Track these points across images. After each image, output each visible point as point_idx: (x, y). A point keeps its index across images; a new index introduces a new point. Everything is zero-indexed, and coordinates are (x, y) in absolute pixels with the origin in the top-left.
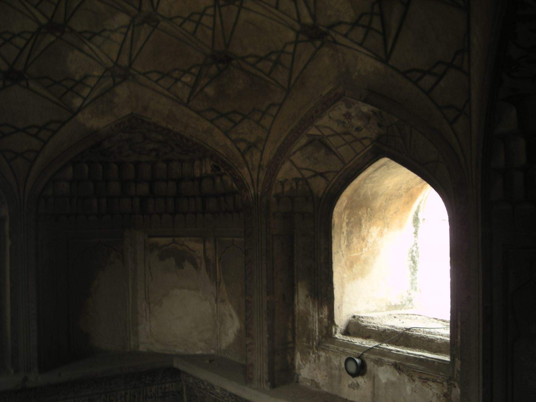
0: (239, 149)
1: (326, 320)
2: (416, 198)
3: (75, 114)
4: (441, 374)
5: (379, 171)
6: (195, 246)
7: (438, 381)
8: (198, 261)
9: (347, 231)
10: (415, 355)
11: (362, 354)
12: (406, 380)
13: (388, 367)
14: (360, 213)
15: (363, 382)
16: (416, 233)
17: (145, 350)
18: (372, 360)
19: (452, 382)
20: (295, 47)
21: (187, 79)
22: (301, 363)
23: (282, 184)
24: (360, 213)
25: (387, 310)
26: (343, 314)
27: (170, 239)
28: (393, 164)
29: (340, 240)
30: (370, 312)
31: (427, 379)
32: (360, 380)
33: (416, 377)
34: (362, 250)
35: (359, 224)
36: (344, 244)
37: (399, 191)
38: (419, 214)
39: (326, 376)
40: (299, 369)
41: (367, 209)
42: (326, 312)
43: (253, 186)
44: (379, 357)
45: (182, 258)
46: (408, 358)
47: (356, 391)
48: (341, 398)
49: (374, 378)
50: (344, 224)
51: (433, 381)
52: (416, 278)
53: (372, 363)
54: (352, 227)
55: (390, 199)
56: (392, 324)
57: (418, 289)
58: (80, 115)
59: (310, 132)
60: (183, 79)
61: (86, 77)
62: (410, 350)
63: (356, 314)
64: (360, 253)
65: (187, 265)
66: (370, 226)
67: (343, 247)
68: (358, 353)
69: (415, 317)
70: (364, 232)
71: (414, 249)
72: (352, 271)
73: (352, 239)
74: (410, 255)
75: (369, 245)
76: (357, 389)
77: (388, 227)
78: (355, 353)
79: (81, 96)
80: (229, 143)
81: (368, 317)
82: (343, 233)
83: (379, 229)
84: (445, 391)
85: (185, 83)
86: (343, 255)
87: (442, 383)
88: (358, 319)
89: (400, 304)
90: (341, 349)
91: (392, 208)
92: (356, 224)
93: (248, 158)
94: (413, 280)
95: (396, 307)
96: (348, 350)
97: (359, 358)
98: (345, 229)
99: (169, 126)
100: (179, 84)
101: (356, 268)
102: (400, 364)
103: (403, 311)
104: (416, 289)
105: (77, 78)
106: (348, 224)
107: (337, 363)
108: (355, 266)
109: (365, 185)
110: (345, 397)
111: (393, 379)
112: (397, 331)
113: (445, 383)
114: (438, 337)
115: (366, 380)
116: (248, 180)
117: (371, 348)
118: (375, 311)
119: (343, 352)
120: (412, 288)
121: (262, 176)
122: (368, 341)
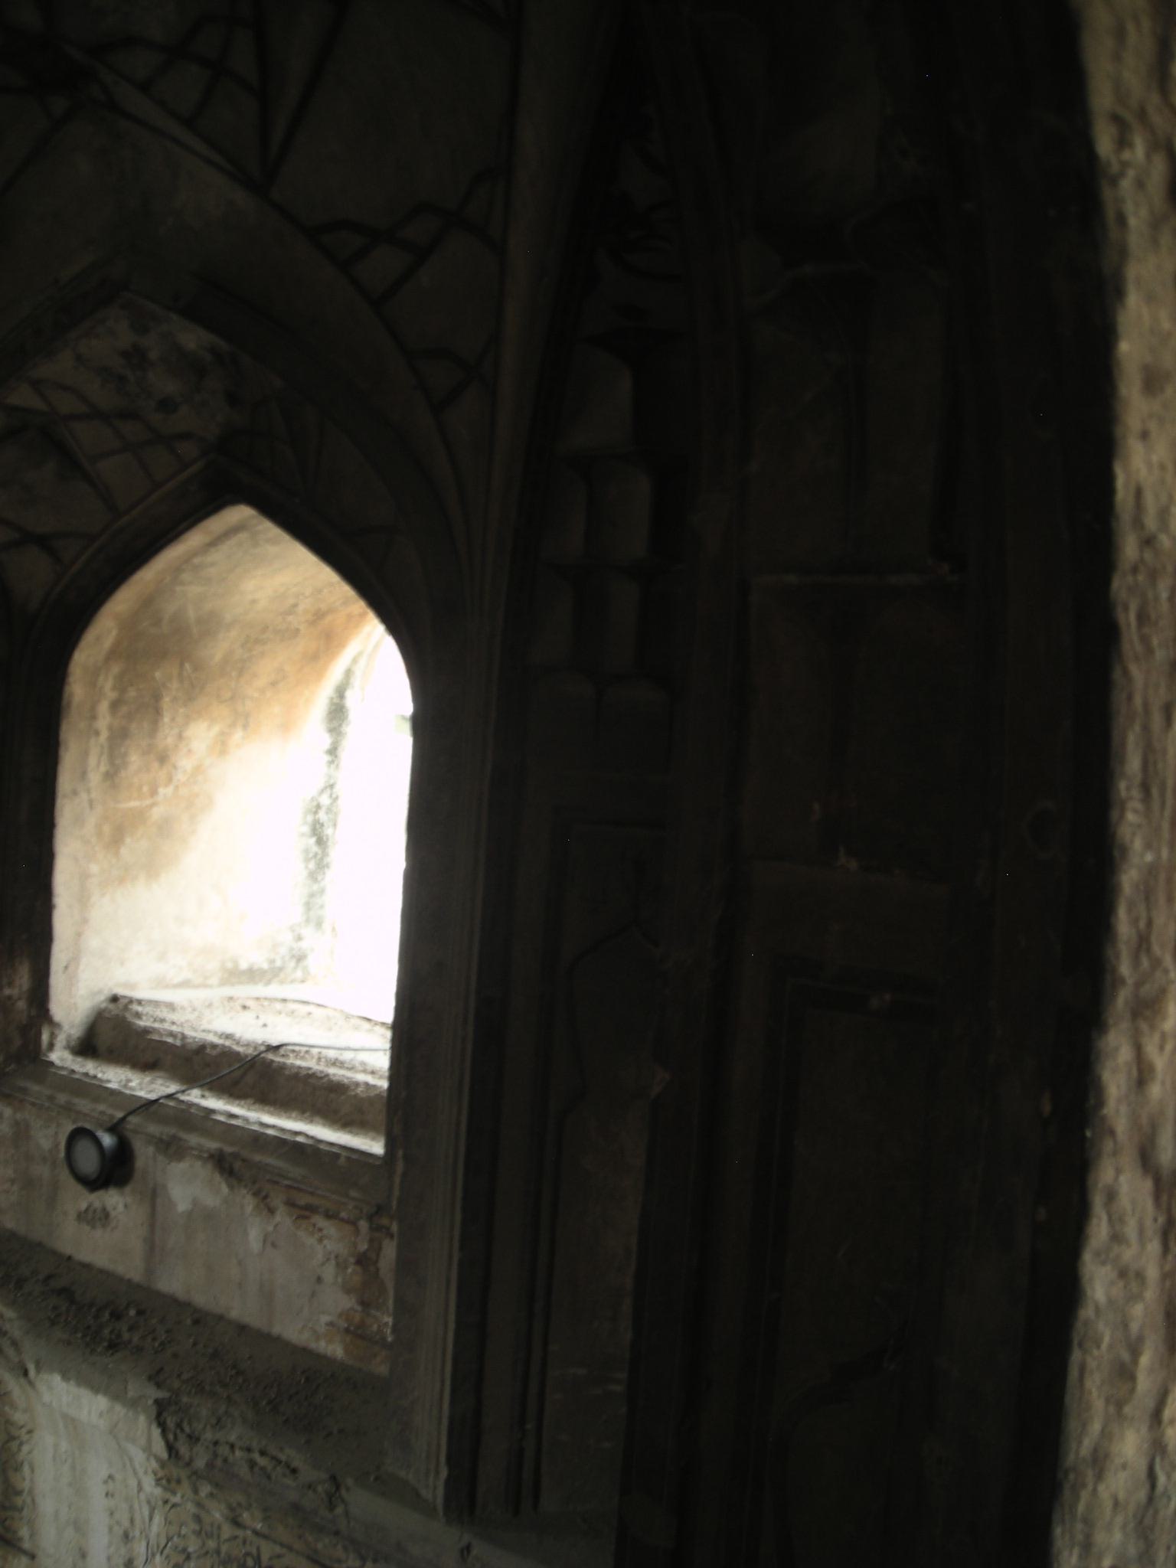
1: (21, 1005)
2: (342, 645)
4: (353, 1193)
5: (225, 548)
7: (343, 1215)
9: (110, 728)
10: (283, 1130)
11: (123, 1119)
12: (249, 1209)
13: (199, 1163)
14: (158, 675)
15: (121, 1208)
16: (333, 751)
18: (151, 1139)
19: (385, 1221)
24: (158, 675)
25: (223, 983)
26: (76, 991)
28: (270, 529)
29: (86, 754)
30: (167, 987)
31: (311, 1209)
32: (113, 1199)
33: (277, 1201)
34: (154, 792)
35: (150, 708)
36: (97, 767)
37: (290, 618)
38: (349, 694)
39: (13, 1181)
41: (182, 665)
42: (23, 978)
44: (171, 1130)
46: (258, 1140)
47: (98, 1233)
48: (54, 1253)
49: (154, 1196)
50: (104, 707)
51: (329, 1216)
52: (322, 891)
53: (151, 1149)
54: (130, 717)
55: (257, 641)
56: (229, 1030)
57: (326, 926)
59: (14, 400)
62: (272, 1114)
63: (121, 991)
64: (148, 802)
66: (188, 719)
67: (95, 778)
68: (112, 1116)
69: (304, 1009)
70: (167, 736)
71: (325, 800)
72: (117, 854)
73: (125, 755)
74: (310, 818)
75: (180, 777)
76: (104, 1226)
77: (245, 727)
78: (102, 1113)
81: (156, 1004)
82: (97, 733)
83: (216, 729)
84: (363, 1247)
86: (91, 803)
87: (353, 1223)
88: (126, 1008)
89: (265, 966)
90: (62, 1098)
91: (264, 669)
92: (141, 709)
94: (312, 895)
95: (252, 975)
96: (83, 1104)
97: (114, 1129)
98: (104, 721)
101: (133, 847)
102: (235, 1156)
103: (274, 990)
104: (319, 924)
106: (115, 706)
107: (46, 1144)
108: (128, 840)
109: (178, 588)
110: (66, 1247)
111: (211, 1201)
112: (238, 1054)
113: (363, 1225)
114: (361, 1077)
115: (129, 1200)
117: (156, 1101)
118: (185, 984)
119: (68, 1109)
120: (308, 921)
122: (148, 1079)
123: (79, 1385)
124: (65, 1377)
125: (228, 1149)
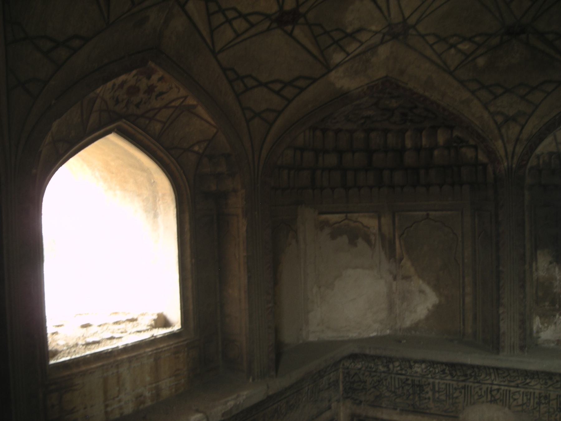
0: (496, 122)
3: (330, 71)
6: (370, 222)
8: (373, 238)
17: (316, 339)
20: (403, 17)
21: (465, 47)
22: (540, 326)
23: (538, 157)
27: (343, 216)
40: (538, 332)
43: (507, 159)
45: (355, 236)
58: (333, 73)
60: (460, 46)
61: (360, 30)
65: (361, 243)
79: (344, 51)
80: (486, 115)
85: (460, 51)
93: (503, 130)
99: (427, 94)
100: (453, 51)
105: (349, 30)
116: (502, 152)
121: (519, 149)
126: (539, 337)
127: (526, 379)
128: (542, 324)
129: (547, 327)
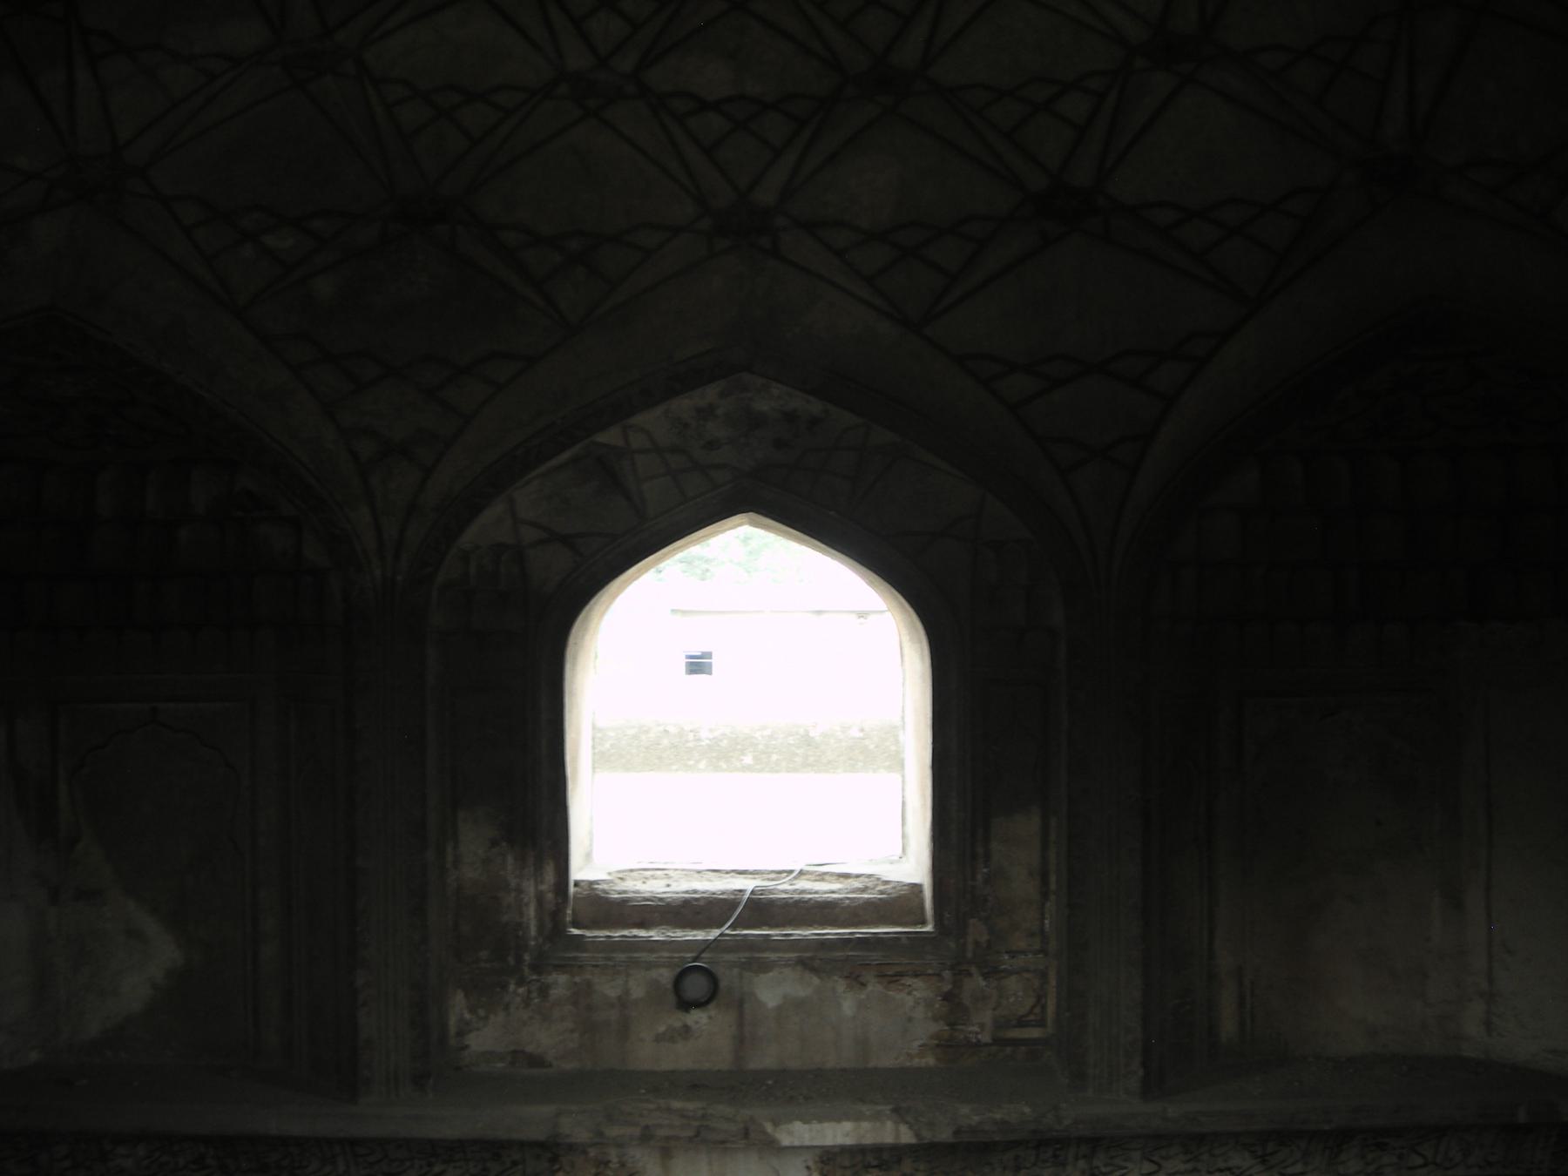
1: (550, 896)
13: (787, 971)
22: (467, 1016)
31: (901, 975)
39: (572, 1031)
40: (460, 1034)
44: (747, 955)
49: (740, 1004)
51: (916, 976)
84: (947, 987)
87: (939, 975)
102: (812, 958)
111: (801, 991)
113: (947, 974)
123: (820, 1121)
124: (805, 1122)
125: (808, 955)
126: (467, 1047)
127: (430, 1165)
128: (472, 1010)
129: (486, 1018)
